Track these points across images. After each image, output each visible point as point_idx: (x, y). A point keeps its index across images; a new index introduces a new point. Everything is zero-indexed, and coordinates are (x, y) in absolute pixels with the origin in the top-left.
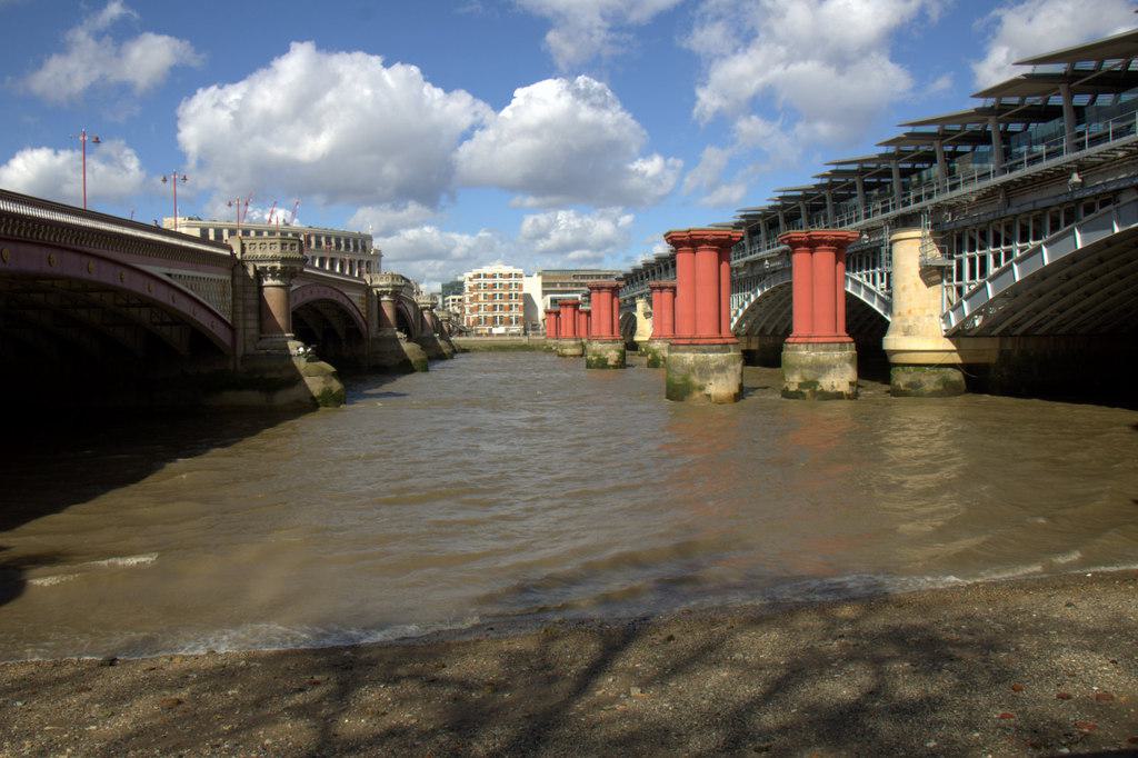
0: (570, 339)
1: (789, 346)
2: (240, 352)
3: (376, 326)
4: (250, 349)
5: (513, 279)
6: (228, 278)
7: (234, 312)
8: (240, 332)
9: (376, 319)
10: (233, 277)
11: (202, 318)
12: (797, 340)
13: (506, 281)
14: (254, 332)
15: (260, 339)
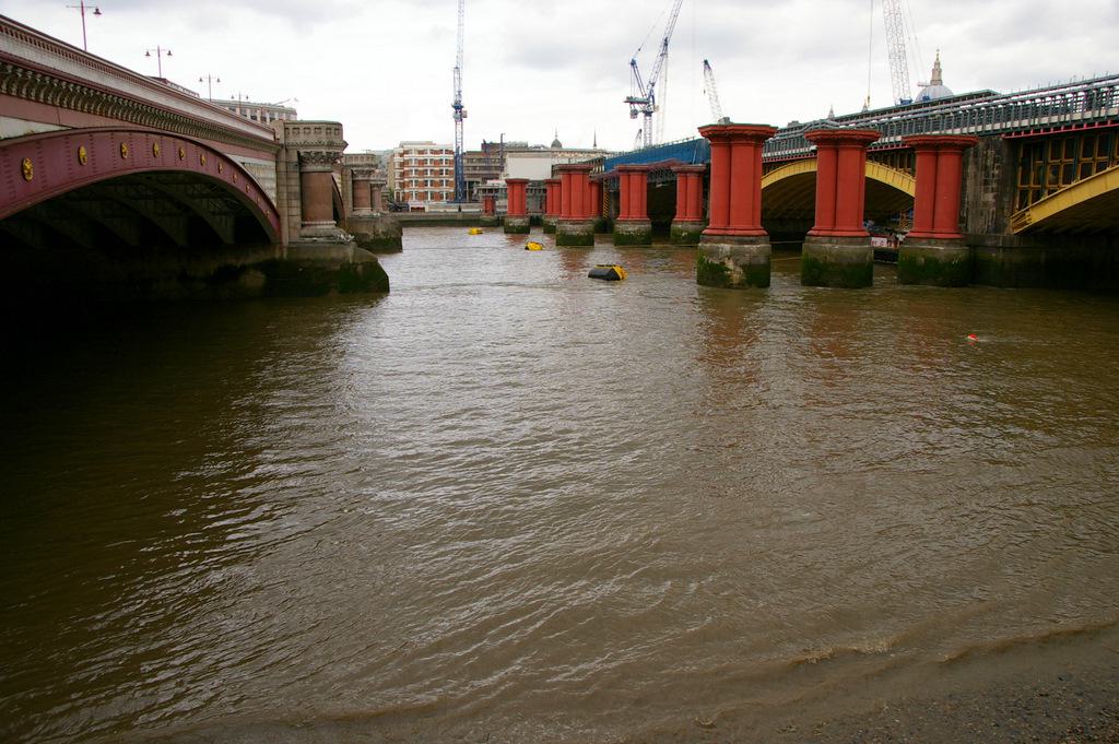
0: (518, 217)
1: (813, 239)
2: (285, 241)
3: (351, 203)
4: (296, 237)
5: (444, 155)
6: (273, 164)
7: (278, 199)
8: (285, 220)
9: (351, 199)
10: (277, 162)
11: (262, 205)
12: (821, 233)
13: (437, 157)
14: (298, 219)
15: (303, 226)
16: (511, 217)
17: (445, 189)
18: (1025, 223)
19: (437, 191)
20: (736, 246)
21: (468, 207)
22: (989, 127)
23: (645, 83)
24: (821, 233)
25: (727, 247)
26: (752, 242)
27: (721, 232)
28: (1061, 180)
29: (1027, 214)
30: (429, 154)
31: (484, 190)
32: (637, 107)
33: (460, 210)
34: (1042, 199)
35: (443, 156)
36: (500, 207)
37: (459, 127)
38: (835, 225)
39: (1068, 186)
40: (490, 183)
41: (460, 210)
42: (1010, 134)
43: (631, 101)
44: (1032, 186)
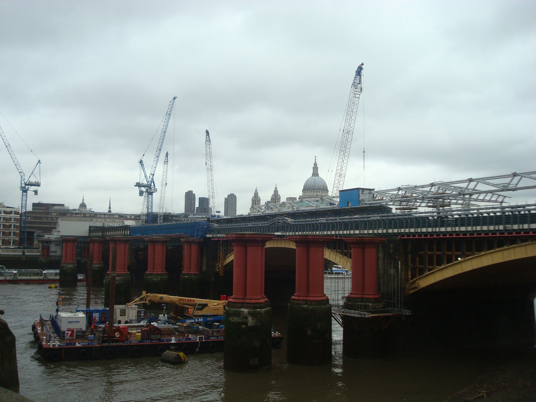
5: (13, 215)
13: (8, 216)
16: (65, 263)
17: (12, 237)
18: (416, 288)
19: (7, 239)
20: (251, 310)
21: (29, 252)
22: (390, 231)
23: (148, 174)
24: (301, 298)
25: (246, 311)
26: (262, 308)
27: (242, 301)
28: (435, 264)
29: (417, 282)
30: (3, 214)
31: (43, 242)
32: (143, 189)
33: (24, 253)
34: (425, 274)
35: (13, 215)
36: (52, 252)
37: (24, 197)
38: (308, 293)
39: (440, 268)
40: (47, 236)
41: (24, 253)
42: (404, 236)
43: (138, 185)
44: (418, 265)
